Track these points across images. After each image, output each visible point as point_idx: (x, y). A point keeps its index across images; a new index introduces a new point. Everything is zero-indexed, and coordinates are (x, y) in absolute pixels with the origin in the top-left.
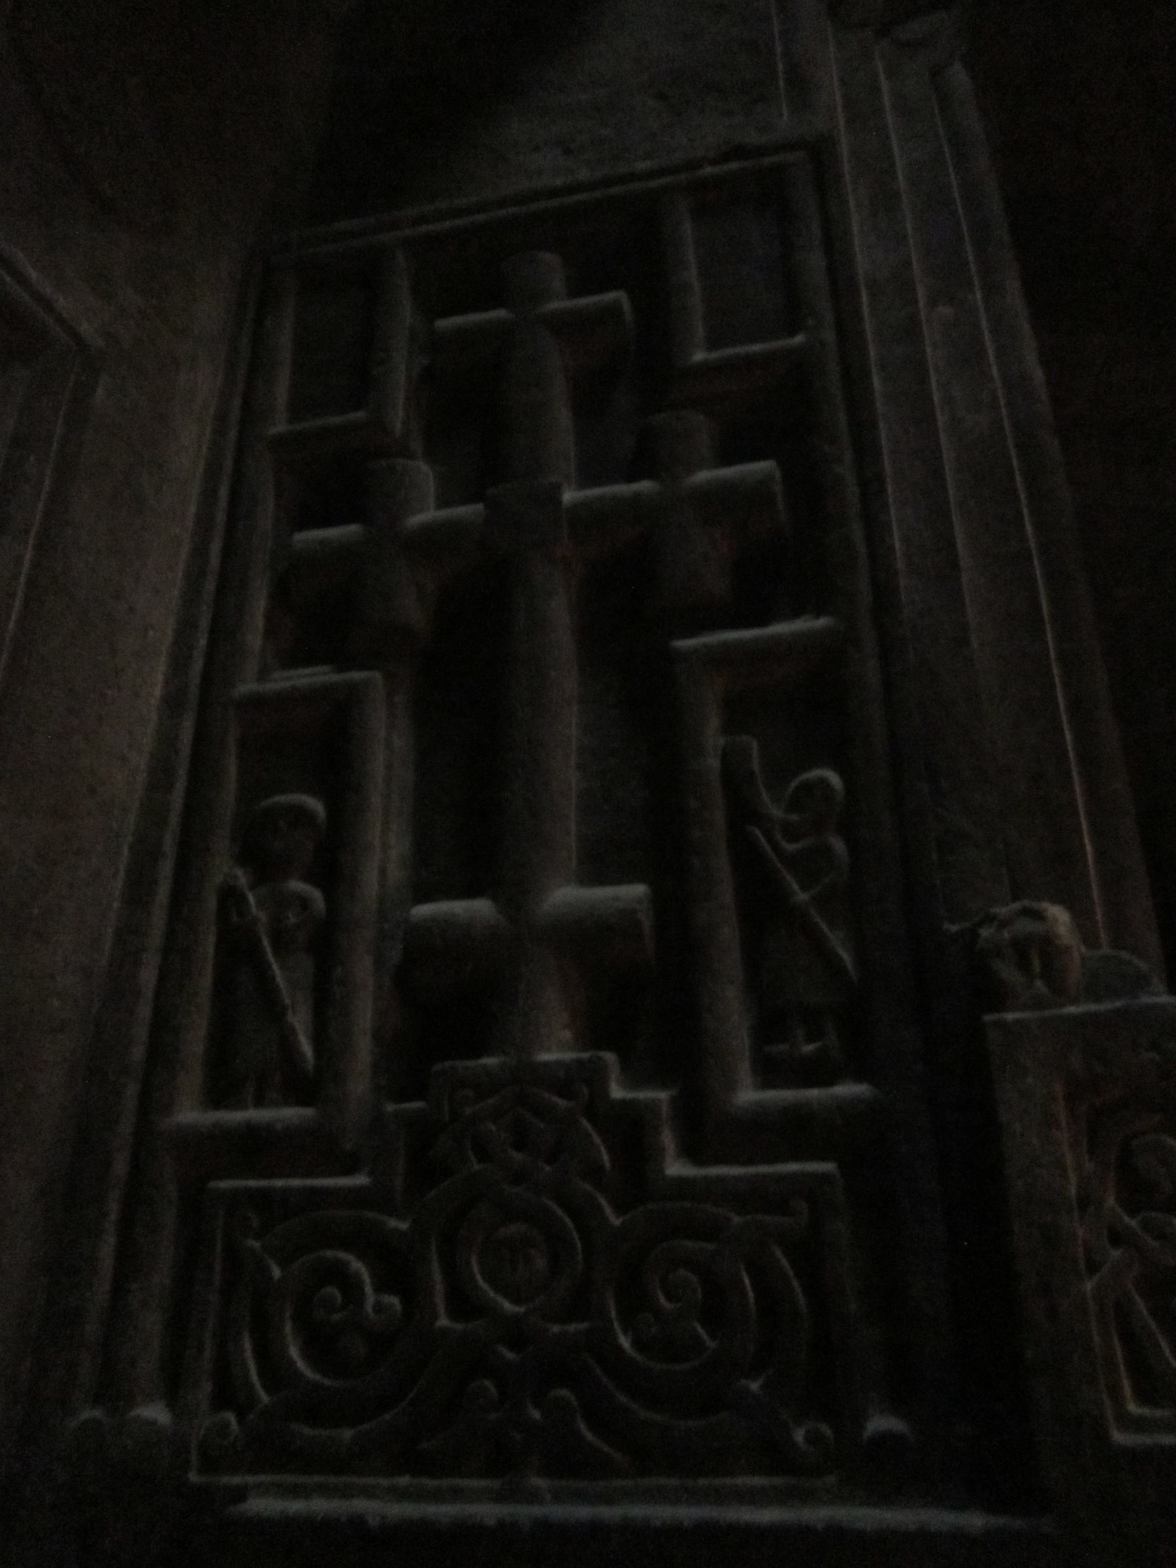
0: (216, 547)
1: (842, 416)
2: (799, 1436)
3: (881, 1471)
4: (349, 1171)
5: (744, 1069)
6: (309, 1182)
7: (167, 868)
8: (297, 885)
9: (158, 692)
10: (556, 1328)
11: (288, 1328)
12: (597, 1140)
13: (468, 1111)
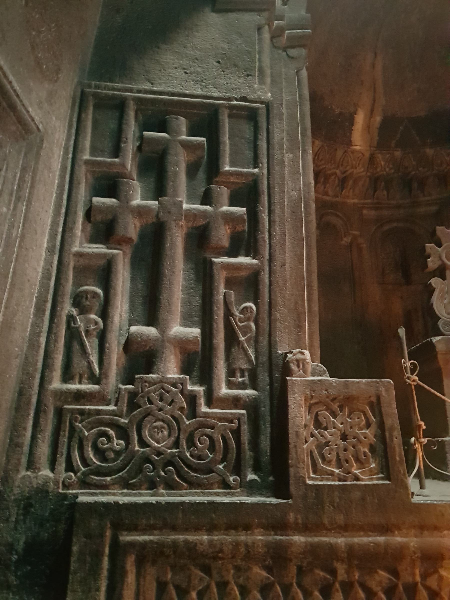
0: (65, 197)
1: (266, 198)
6: (97, 407)
8: (93, 316)
9: (45, 245)
10: (169, 451)
11: (90, 449)
13: (147, 389)
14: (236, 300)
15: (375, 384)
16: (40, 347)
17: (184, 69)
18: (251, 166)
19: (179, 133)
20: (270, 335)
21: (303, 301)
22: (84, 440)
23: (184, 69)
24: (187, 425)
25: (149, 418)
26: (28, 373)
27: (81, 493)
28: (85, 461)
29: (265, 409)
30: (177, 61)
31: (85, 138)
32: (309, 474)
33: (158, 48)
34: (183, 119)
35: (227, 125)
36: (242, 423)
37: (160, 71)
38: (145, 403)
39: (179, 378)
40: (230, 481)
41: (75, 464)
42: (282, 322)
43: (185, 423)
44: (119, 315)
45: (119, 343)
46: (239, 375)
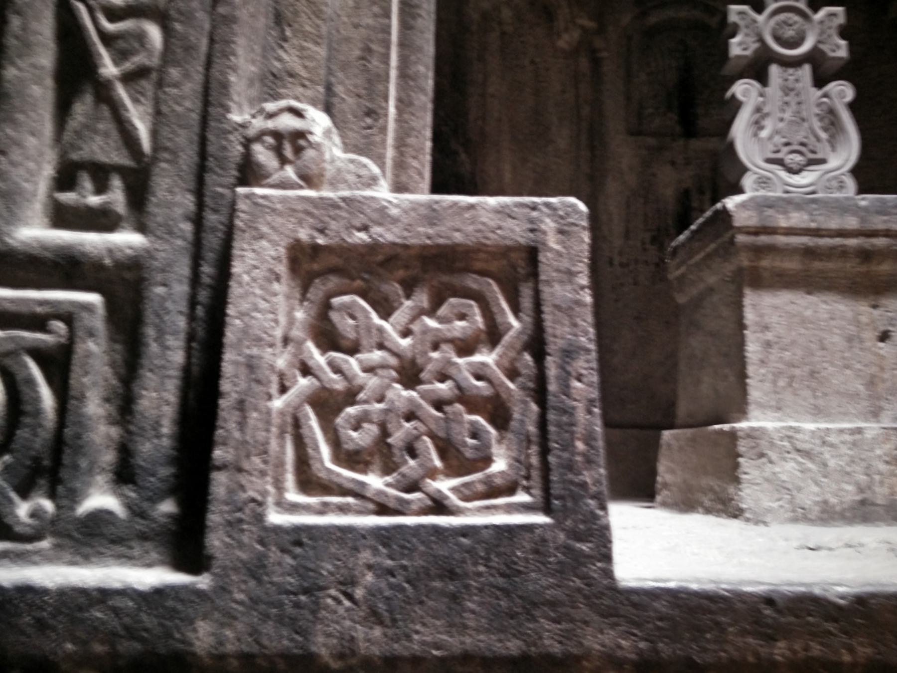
3: (92, 537)
15: (527, 210)
21: (387, 44)
36: (80, 333)
42: (307, 83)
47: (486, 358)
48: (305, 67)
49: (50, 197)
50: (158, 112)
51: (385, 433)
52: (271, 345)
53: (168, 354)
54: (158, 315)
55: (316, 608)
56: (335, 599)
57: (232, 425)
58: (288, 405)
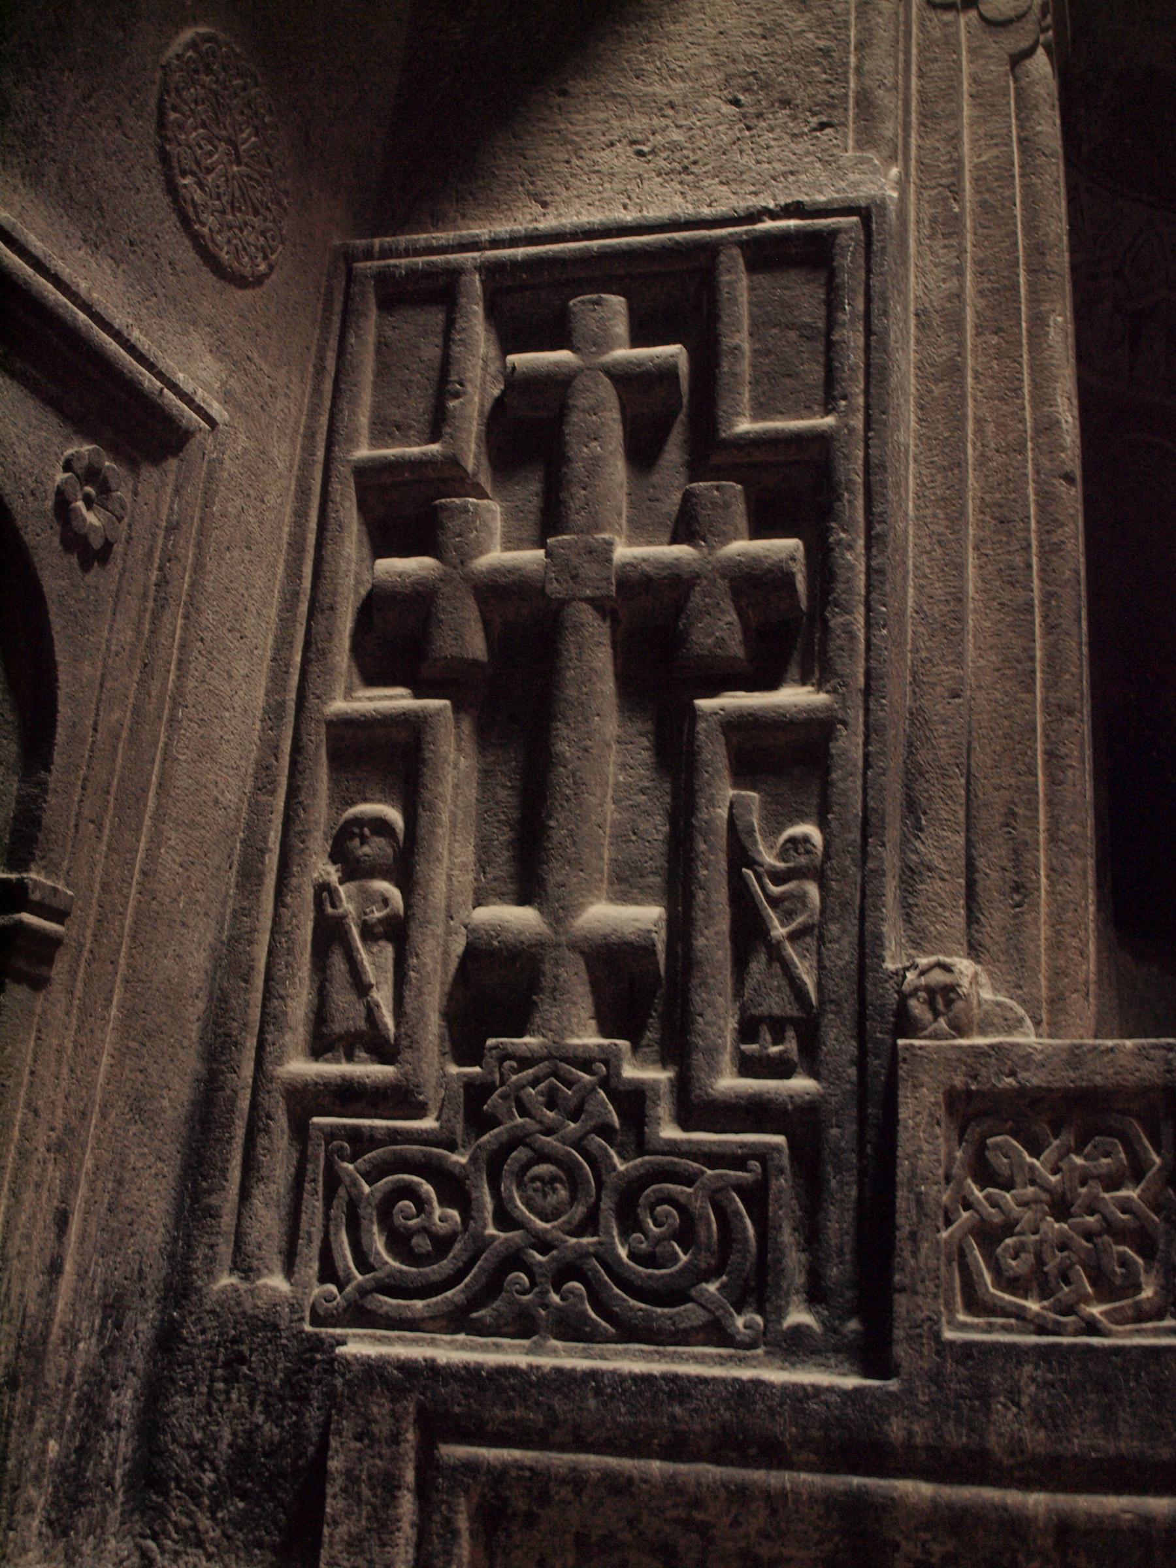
0: (308, 570)
1: (860, 502)
2: (740, 1322)
3: (793, 1348)
4: (420, 1116)
5: (726, 1060)
7: (272, 861)
10: (573, 1240)
11: (375, 1228)
12: (611, 1107)
14: (764, 818)
15: (1163, 1052)
16: (252, 968)
17: (633, 142)
18: (816, 408)
19: (604, 343)
20: (862, 918)
22: (362, 1205)
23: (633, 142)
24: (621, 1175)
25: (520, 1154)
26: (229, 1036)
27: (355, 1336)
28: (364, 1262)
29: (840, 1135)
30: (615, 123)
31: (354, 402)
32: (952, 1312)
33: (564, 93)
34: (617, 302)
35: (744, 298)
37: (568, 162)
38: (512, 1117)
39: (599, 1046)
40: (734, 1325)
41: (340, 1265)
42: (947, 877)
43: (614, 1168)
44: (444, 877)
45: (446, 953)
46: (768, 1037)
47: (1131, 1193)
48: (944, 859)
49: (737, 1048)
50: (821, 967)
51: (1040, 1261)
52: (936, 1183)
53: (843, 1189)
54: (835, 1155)
55: (988, 1410)
56: (1004, 1405)
57: (906, 1254)
58: (951, 1236)
